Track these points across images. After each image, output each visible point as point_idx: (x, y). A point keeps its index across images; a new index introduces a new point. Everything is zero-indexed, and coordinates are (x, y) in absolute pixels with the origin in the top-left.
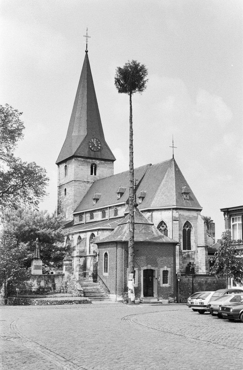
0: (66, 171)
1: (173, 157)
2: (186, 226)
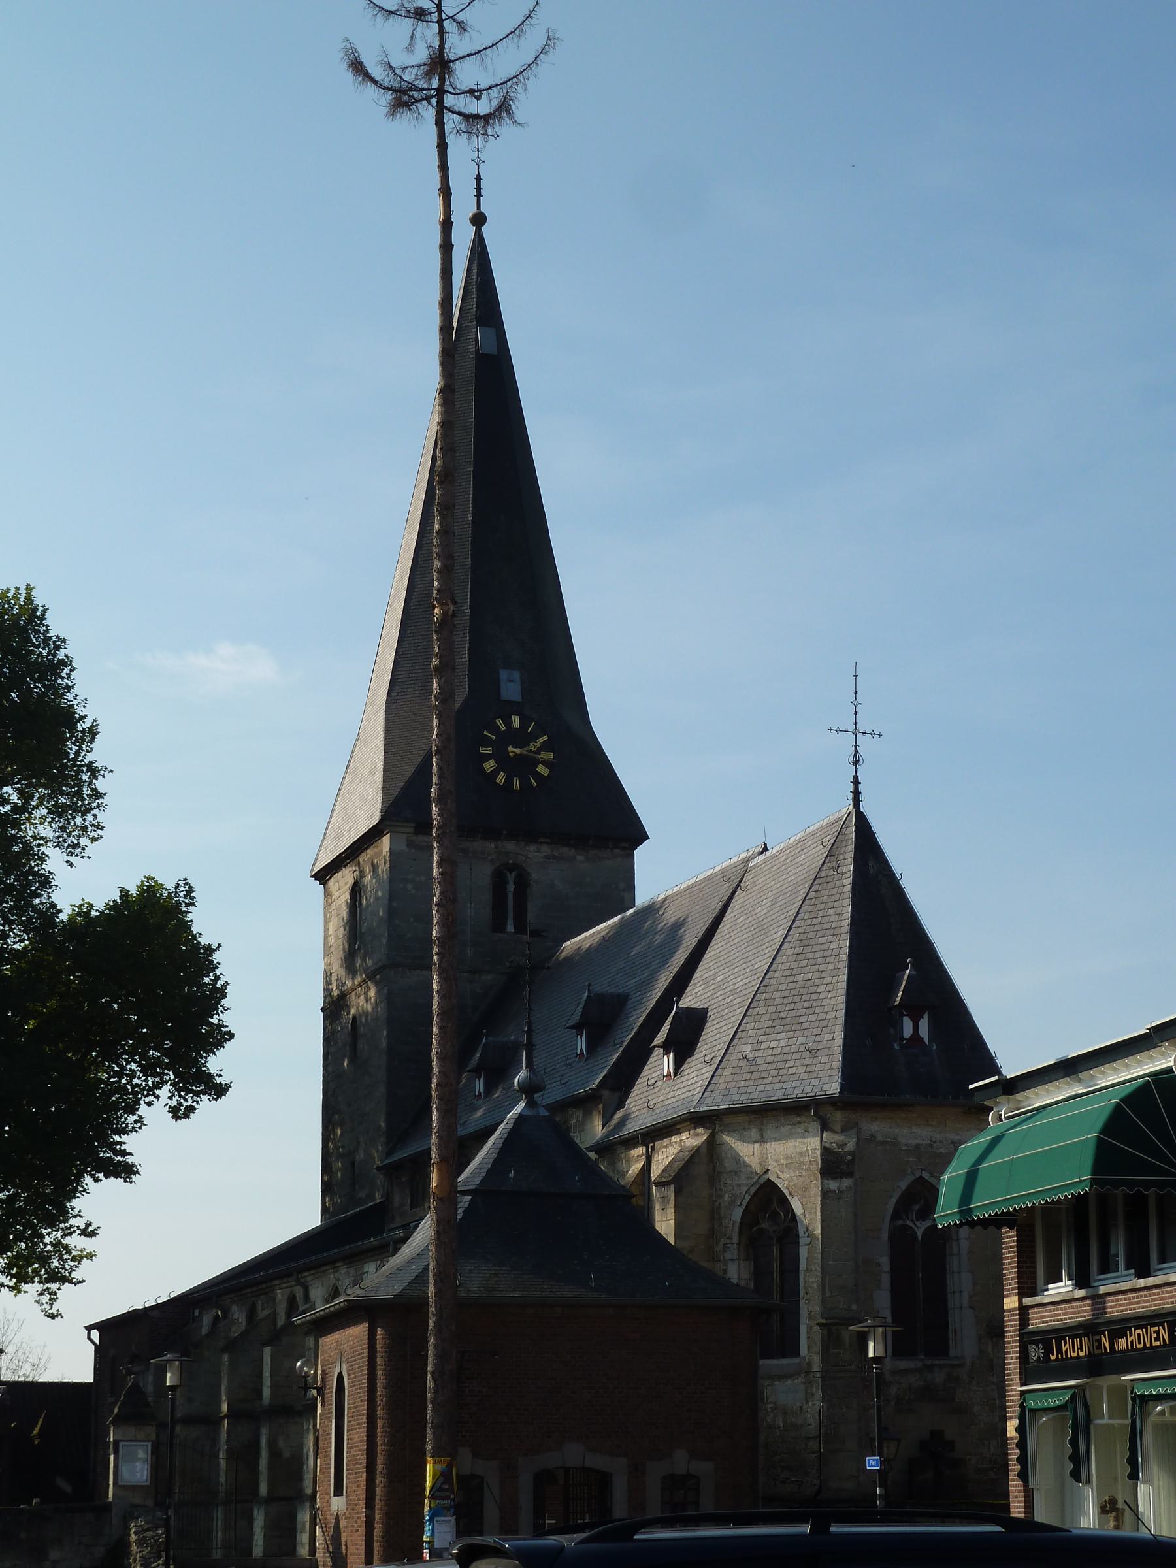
1: (856, 793)
2: (916, 1207)
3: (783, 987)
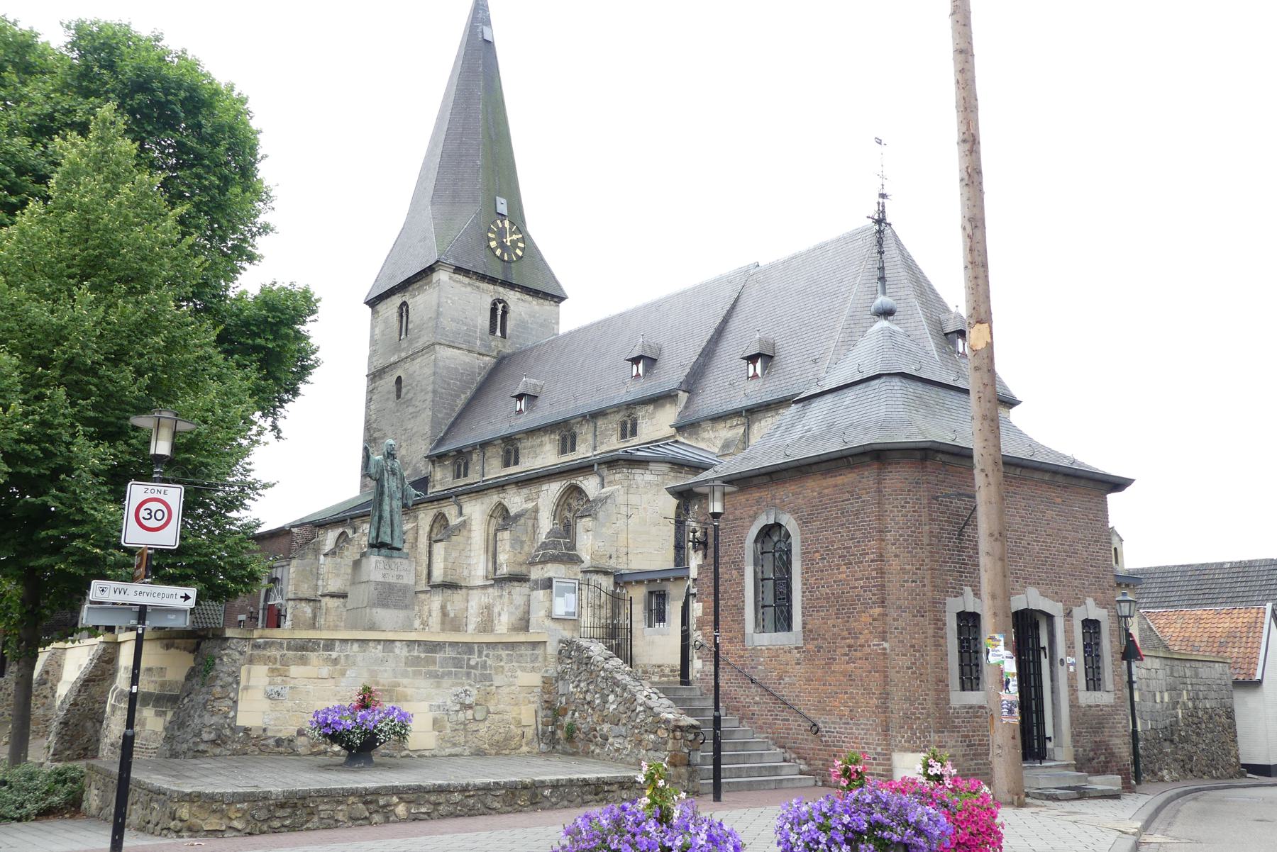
0: (401, 322)
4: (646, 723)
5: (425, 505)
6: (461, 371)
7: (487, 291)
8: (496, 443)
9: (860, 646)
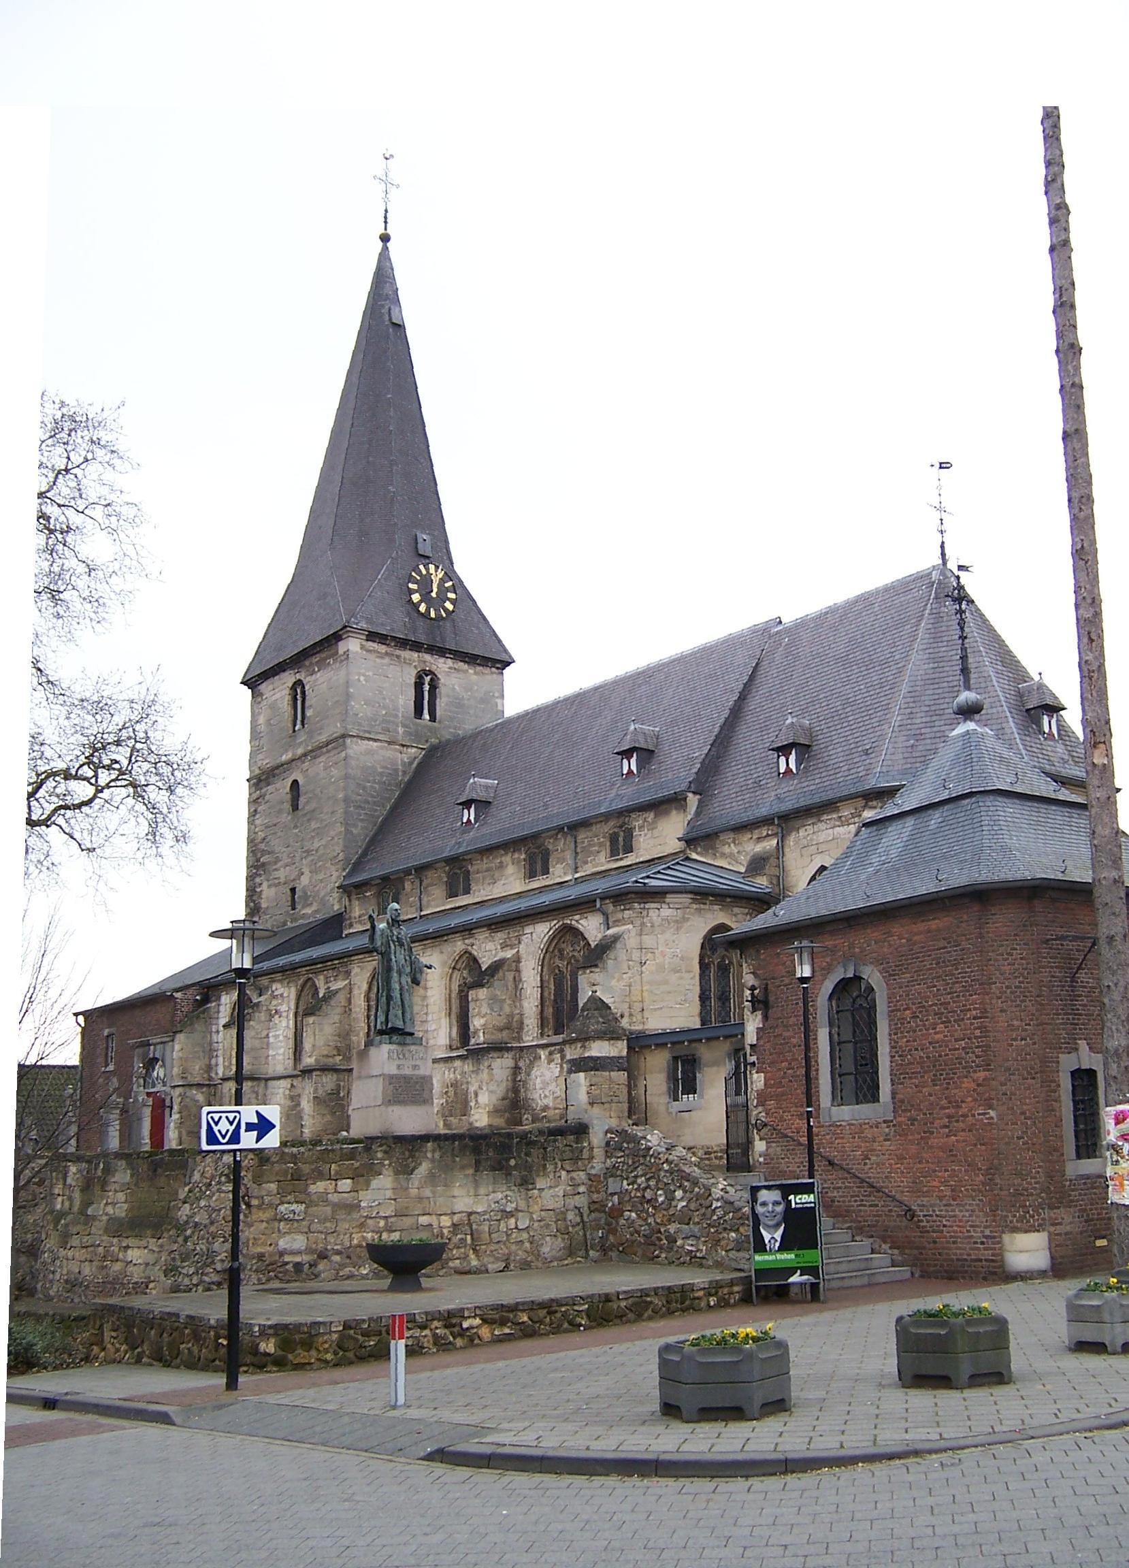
3: (930, 692)
4: (725, 1221)
5: (360, 957)
6: (380, 770)
7: (409, 663)
8: (437, 865)
9: (962, 1116)
